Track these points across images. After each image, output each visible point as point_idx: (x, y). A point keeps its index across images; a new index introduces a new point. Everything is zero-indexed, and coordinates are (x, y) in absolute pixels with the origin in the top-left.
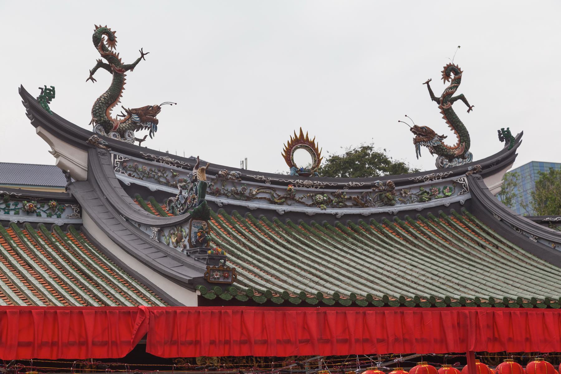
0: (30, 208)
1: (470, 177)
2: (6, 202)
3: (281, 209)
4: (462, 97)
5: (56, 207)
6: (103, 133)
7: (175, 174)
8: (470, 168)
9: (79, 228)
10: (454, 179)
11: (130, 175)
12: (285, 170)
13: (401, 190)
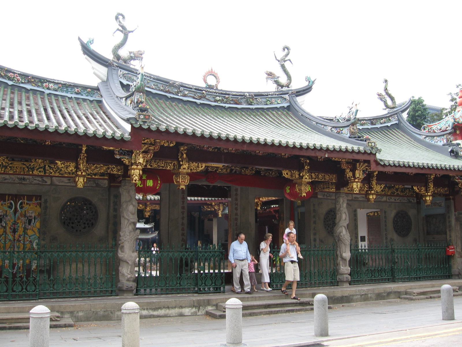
0: (78, 91)
1: (290, 96)
2: (67, 87)
3: (198, 102)
4: (290, 60)
5: (90, 92)
6: (116, 60)
7: (148, 81)
8: (290, 92)
9: (100, 102)
10: (282, 96)
11: (127, 80)
12: (203, 85)
13: (257, 98)
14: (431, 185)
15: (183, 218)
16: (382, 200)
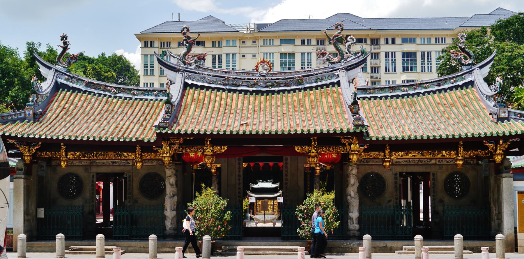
10: (333, 72)
14: (461, 150)
15: (239, 184)
16: (431, 163)
